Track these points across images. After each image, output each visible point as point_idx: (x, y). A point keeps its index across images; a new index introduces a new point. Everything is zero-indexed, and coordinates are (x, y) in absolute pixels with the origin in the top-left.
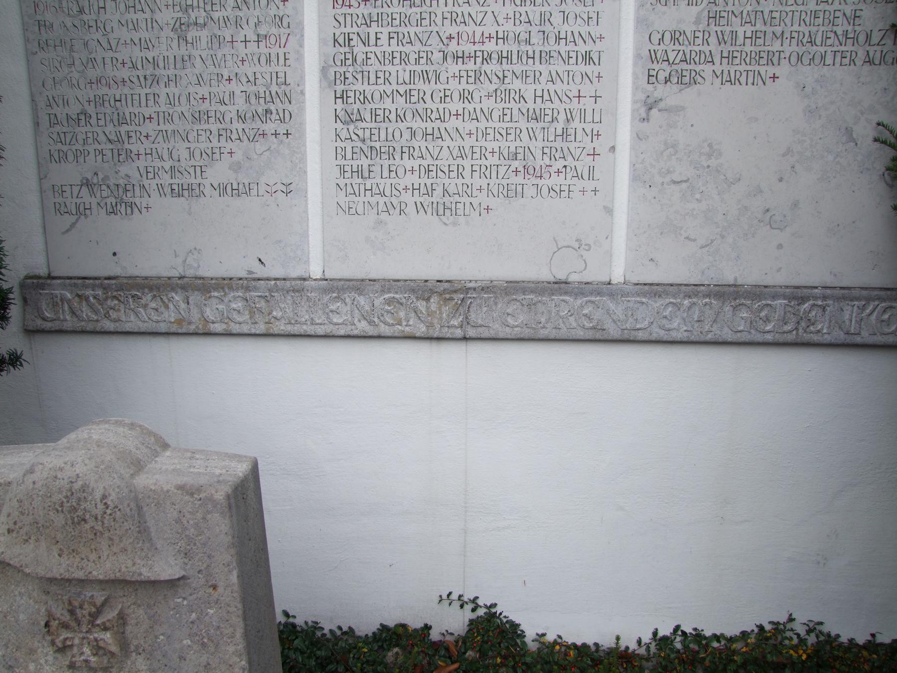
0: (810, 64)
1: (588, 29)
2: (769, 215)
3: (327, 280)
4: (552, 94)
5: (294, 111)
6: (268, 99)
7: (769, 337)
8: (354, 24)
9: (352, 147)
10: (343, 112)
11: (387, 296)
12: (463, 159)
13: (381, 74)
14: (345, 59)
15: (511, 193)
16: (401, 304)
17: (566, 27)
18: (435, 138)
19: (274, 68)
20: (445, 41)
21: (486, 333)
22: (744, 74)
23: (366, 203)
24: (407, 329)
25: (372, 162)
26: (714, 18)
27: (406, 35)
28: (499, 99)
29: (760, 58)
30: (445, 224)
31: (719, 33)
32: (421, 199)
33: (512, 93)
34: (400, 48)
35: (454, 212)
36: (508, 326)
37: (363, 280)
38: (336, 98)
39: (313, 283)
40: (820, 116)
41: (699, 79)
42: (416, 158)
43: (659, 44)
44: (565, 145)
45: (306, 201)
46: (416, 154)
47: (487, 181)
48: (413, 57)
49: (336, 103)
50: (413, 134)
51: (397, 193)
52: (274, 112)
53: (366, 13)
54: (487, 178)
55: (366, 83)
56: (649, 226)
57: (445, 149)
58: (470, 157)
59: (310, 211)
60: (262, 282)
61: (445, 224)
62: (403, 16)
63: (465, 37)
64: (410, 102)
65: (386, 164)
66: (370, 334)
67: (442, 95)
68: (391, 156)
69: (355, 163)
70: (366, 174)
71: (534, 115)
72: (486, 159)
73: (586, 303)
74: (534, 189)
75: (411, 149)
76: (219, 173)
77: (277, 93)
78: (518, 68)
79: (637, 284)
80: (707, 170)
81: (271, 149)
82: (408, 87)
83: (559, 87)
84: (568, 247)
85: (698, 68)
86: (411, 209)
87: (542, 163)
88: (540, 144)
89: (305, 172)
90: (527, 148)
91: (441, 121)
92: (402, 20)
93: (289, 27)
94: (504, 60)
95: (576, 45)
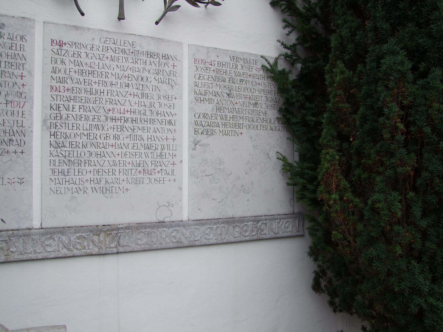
0: (253, 129)
1: (170, 110)
2: (243, 187)
3: (43, 229)
4: (155, 137)
5: (26, 140)
6: (11, 133)
7: (247, 238)
8: (62, 100)
9: (59, 160)
10: (54, 142)
11: (77, 235)
12: (115, 166)
13: (75, 125)
14: (56, 116)
15: (137, 182)
16: (85, 238)
17: (161, 109)
18: (101, 156)
19: (15, 118)
20: (107, 112)
21: (128, 249)
22: (231, 132)
23: (66, 188)
24: (89, 251)
25: (69, 168)
26: (219, 109)
27: (88, 107)
28: (132, 139)
29: (236, 126)
30: (107, 197)
31: (221, 115)
32: (95, 186)
33: (138, 136)
34: (85, 113)
35: (111, 192)
36: (139, 245)
37: (64, 228)
38: (51, 135)
39: (36, 231)
40: (258, 149)
41: (214, 133)
42: (92, 165)
43: (198, 118)
44: (161, 160)
45: (32, 187)
46: (92, 164)
47: (126, 177)
48: (91, 118)
49: (50, 138)
50: (91, 154)
51: (82, 183)
52: (15, 140)
53: (68, 95)
54: (126, 175)
55: (67, 129)
56: (198, 194)
57: (106, 161)
58: (118, 165)
59: (33, 192)
60: (4, 232)
61: (107, 197)
62: (87, 98)
63: (116, 110)
64: (89, 139)
65: (77, 168)
66: (69, 255)
67: (105, 136)
68: (79, 165)
69: (60, 168)
70: (66, 174)
71: (147, 147)
72: (126, 166)
73: (174, 230)
74: (148, 181)
75: (90, 161)
77: (17, 131)
78: (140, 126)
79: (194, 220)
80: (219, 170)
81: (12, 160)
82: (89, 132)
83: (158, 134)
84: (164, 206)
85: (214, 129)
86: (89, 190)
87: (151, 168)
88: (150, 159)
89: (32, 172)
90: (144, 161)
91: (105, 148)
92: (86, 100)
93: (25, 98)
94: (134, 122)
95: (165, 117)
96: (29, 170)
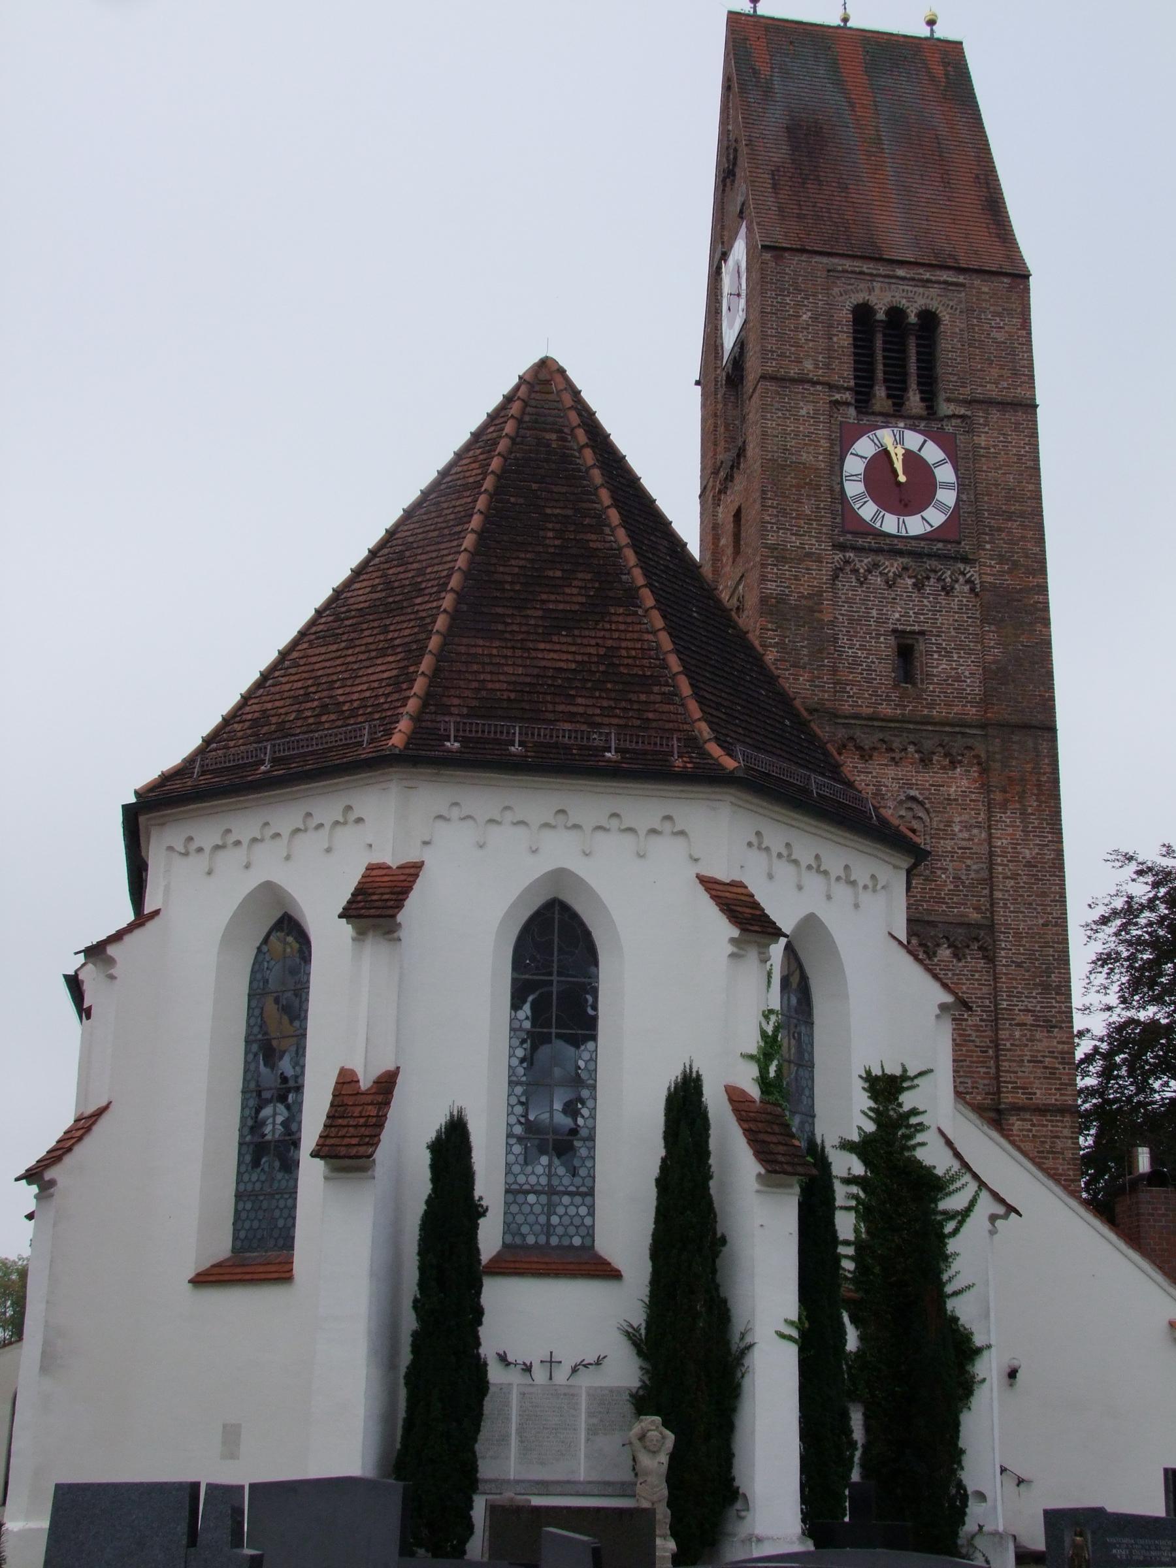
26: (601, 1421)
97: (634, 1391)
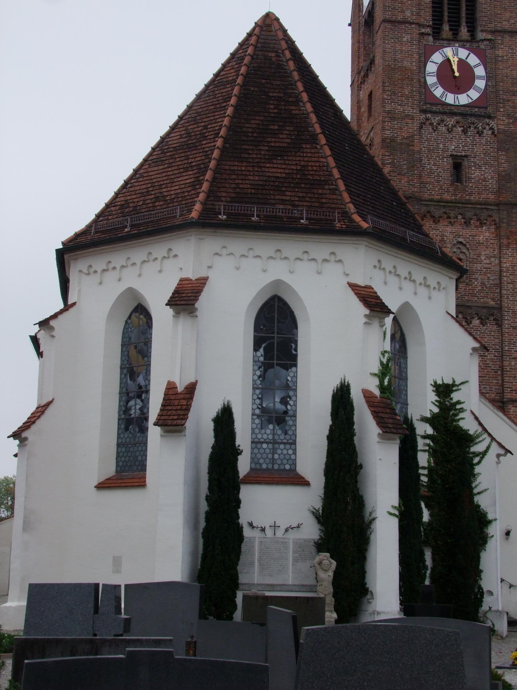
26: (300, 555)
76: (245, 571)
96: (255, 571)
97: (316, 541)
